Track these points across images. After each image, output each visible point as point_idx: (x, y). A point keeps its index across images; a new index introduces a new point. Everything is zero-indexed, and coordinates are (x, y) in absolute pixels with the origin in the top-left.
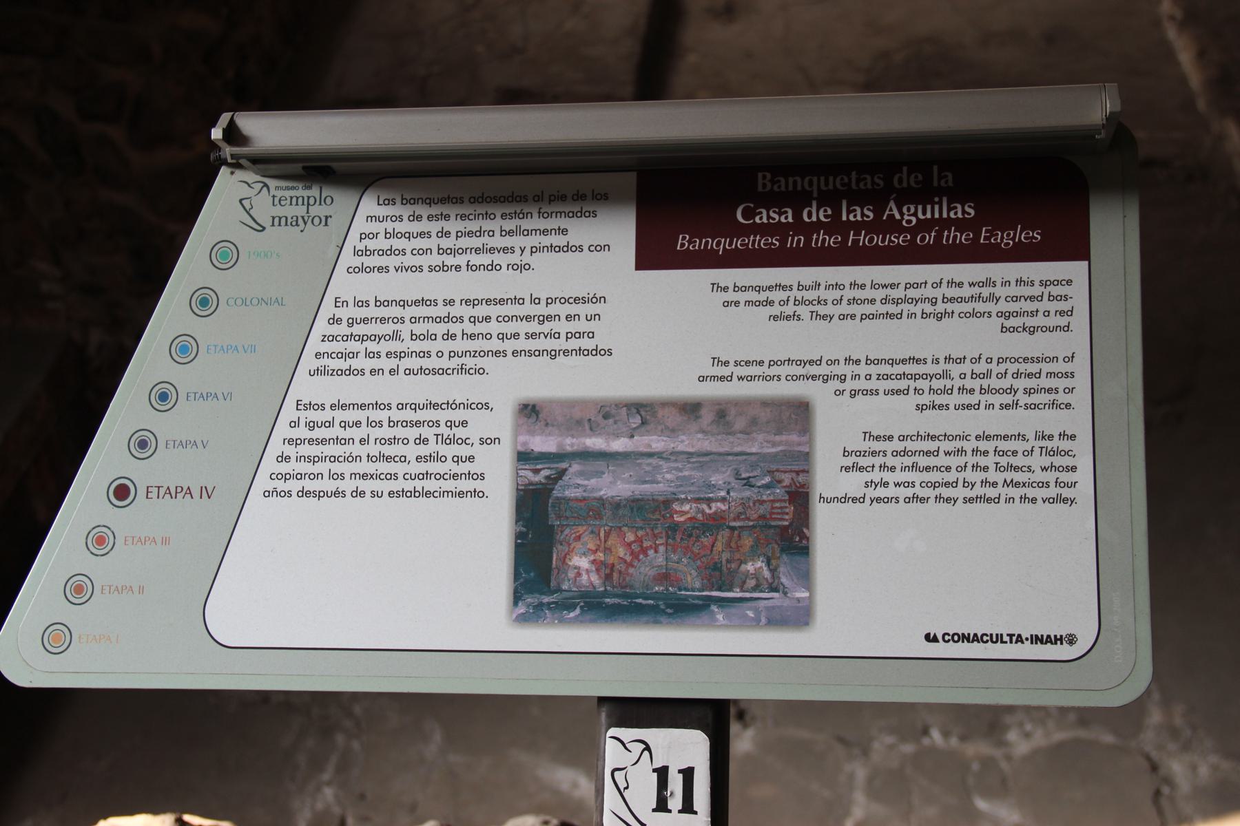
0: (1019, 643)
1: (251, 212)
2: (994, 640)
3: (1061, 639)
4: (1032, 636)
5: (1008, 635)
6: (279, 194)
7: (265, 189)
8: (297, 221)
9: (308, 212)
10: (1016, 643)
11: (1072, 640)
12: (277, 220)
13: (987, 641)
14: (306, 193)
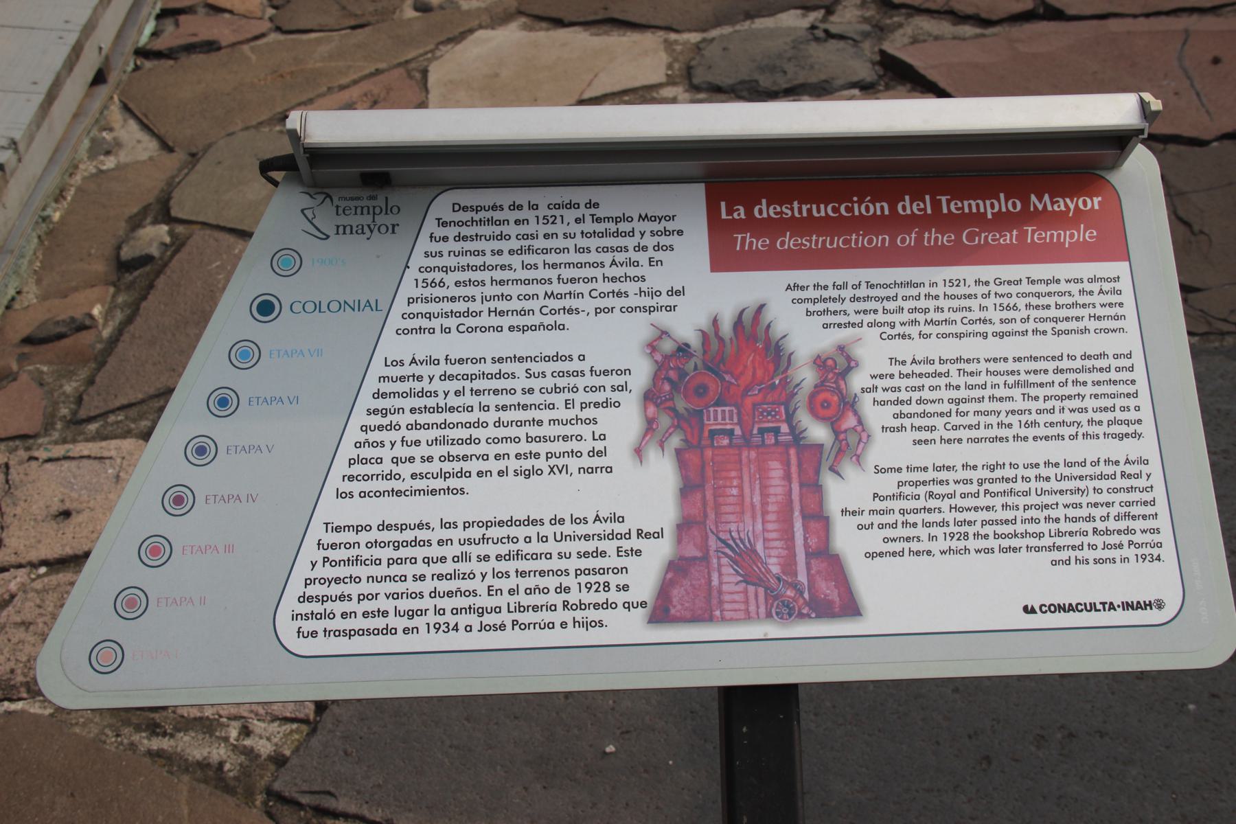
0: (1112, 611)
1: (314, 221)
2: (1088, 608)
3: (1150, 604)
4: (1123, 603)
5: (1101, 603)
6: (343, 204)
7: (328, 199)
8: (363, 229)
9: (374, 221)
10: (1109, 610)
11: (1160, 605)
12: (341, 229)
13: (1082, 610)
14: (371, 203)
